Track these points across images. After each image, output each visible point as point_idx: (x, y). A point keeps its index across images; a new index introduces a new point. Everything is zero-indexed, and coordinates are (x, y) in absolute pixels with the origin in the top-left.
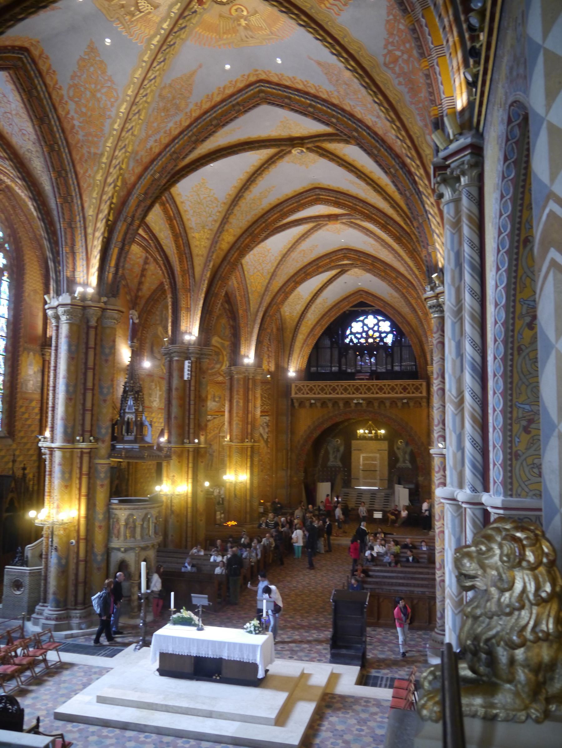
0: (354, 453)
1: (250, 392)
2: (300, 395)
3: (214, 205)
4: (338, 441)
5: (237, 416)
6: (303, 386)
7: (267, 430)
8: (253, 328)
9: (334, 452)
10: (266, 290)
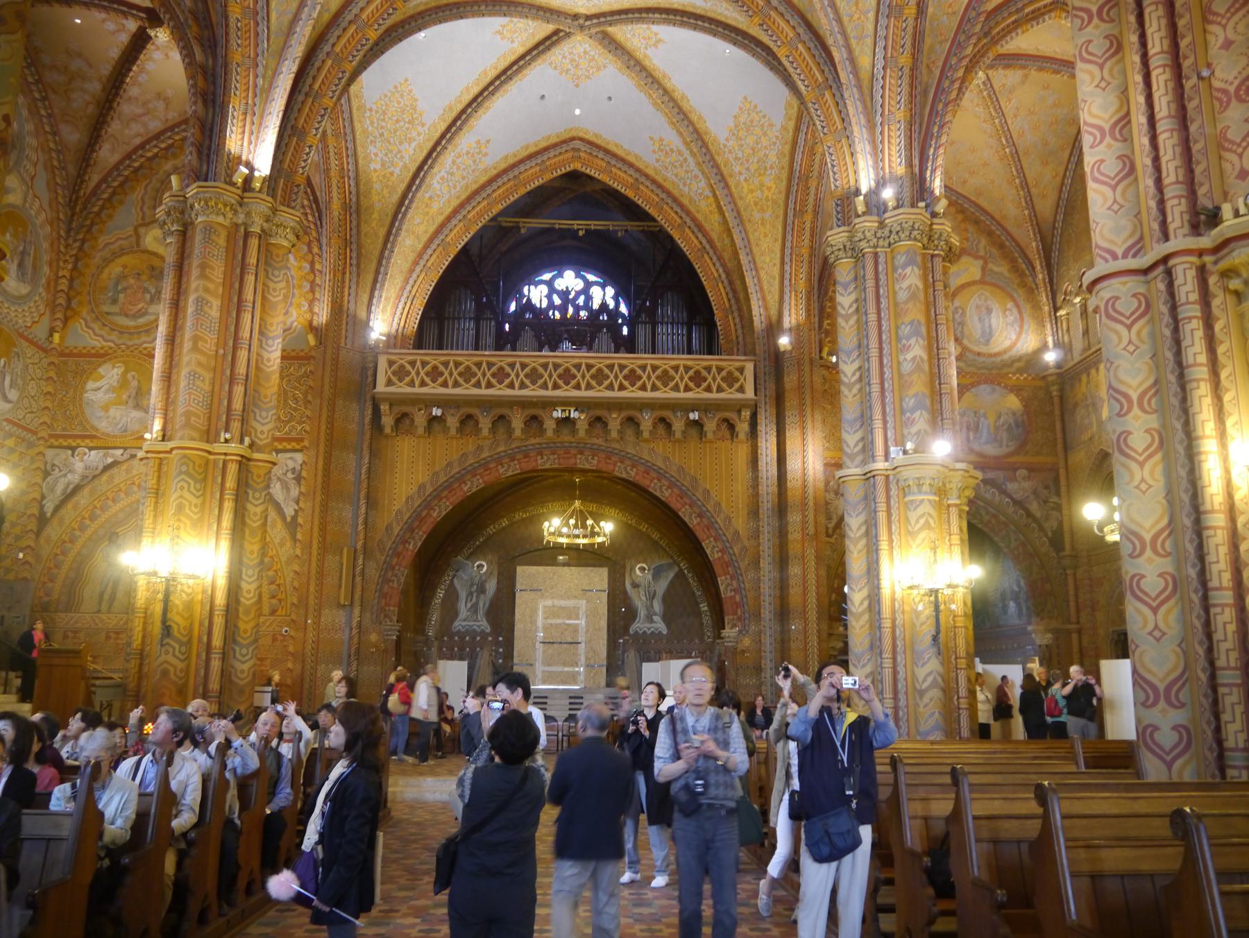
0: (521, 599)
1: (250, 279)
2: (402, 389)
4: (482, 567)
5: (195, 348)
6: (413, 363)
7: (295, 492)
8: (276, 73)
9: (471, 594)
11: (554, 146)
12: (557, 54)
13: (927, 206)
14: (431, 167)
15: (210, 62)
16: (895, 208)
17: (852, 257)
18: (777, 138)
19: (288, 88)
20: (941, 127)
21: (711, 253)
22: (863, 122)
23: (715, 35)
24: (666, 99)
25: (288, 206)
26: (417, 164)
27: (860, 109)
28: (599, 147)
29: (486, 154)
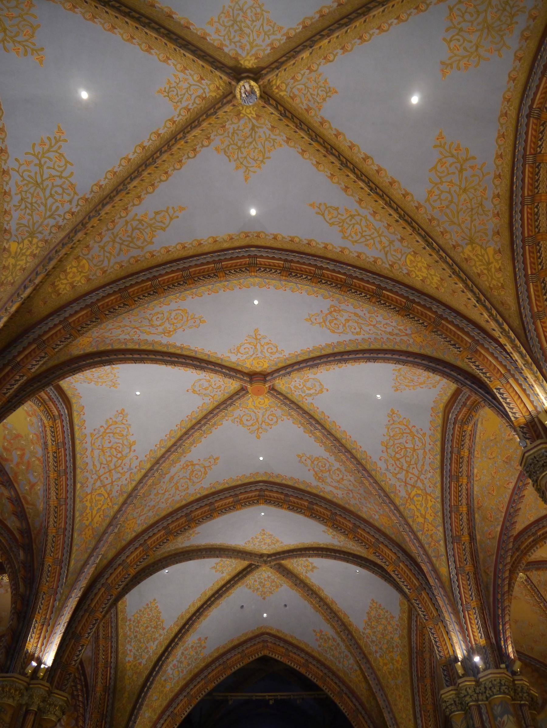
3: (67, 198)
8: (68, 597)
10: (110, 524)
11: (250, 639)
12: (251, 579)
13: (507, 667)
14: (167, 658)
15: (28, 593)
16: (484, 670)
17: (462, 710)
18: (397, 625)
19: (74, 607)
20: (503, 610)
21: (363, 712)
22: (450, 610)
23: (348, 562)
24: (322, 604)
25: (61, 690)
26: (158, 656)
27: (446, 602)
28: (280, 639)
29: (205, 647)
